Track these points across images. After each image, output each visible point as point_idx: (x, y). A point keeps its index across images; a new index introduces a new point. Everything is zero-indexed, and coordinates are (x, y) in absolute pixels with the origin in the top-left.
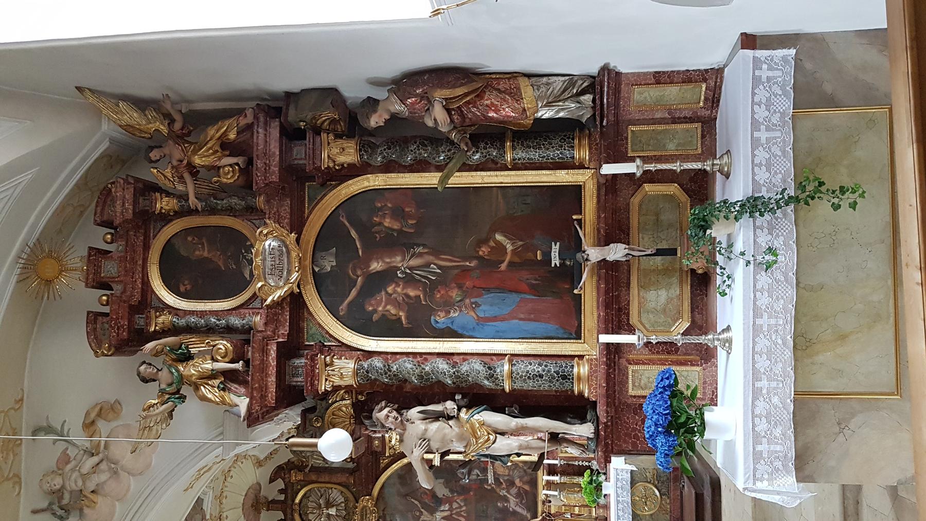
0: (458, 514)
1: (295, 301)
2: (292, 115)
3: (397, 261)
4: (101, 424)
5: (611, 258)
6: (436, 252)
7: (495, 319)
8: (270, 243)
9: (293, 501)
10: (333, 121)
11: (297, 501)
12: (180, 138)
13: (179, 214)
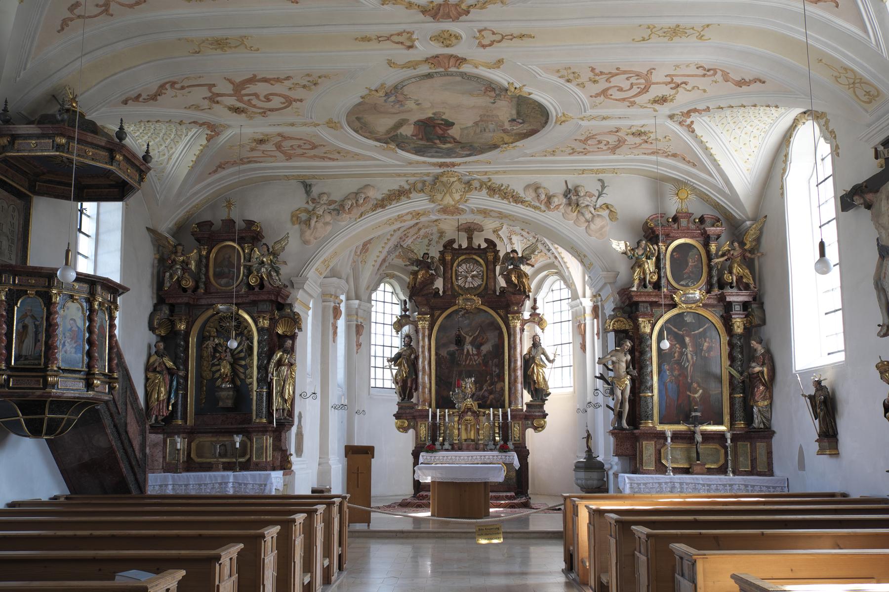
0: (471, 359)
1: (674, 305)
2: (754, 306)
3: (690, 349)
4: (607, 211)
5: (696, 435)
6: (694, 365)
7: (666, 389)
8: (697, 295)
9: (475, 254)
10: (751, 323)
11: (475, 257)
12: (744, 257)
13: (708, 252)
